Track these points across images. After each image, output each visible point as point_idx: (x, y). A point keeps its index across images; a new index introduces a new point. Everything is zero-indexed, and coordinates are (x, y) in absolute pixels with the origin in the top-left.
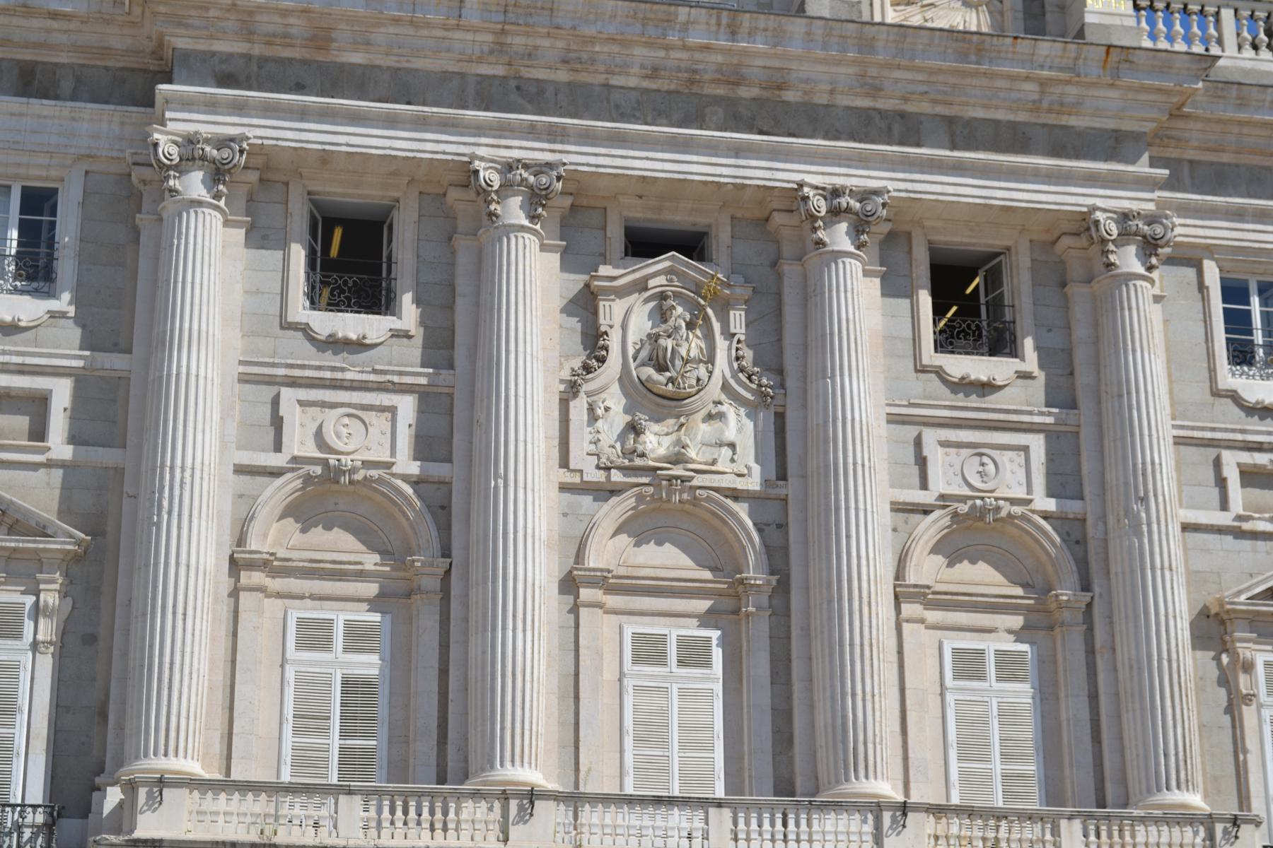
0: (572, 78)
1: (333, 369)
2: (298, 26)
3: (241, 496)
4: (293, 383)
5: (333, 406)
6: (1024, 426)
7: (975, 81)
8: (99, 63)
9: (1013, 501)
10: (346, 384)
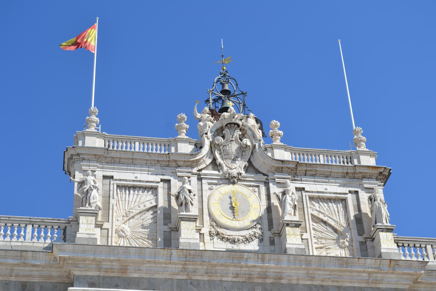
0: (209, 279)
2: (116, 265)
7: (346, 274)
8: (48, 281)
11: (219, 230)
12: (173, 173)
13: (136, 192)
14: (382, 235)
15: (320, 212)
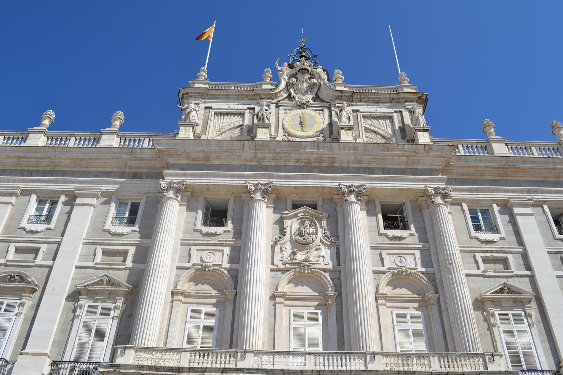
1: (207, 240)
3: (177, 275)
4: (195, 245)
5: (206, 250)
6: (413, 248)
7: (388, 157)
8: (153, 171)
9: (411, 269)
10: (210, 245)
11: (290, 138)
12: (257, 103)
13: (229, 117)
14: (420, 134)
15: (371, 125)
